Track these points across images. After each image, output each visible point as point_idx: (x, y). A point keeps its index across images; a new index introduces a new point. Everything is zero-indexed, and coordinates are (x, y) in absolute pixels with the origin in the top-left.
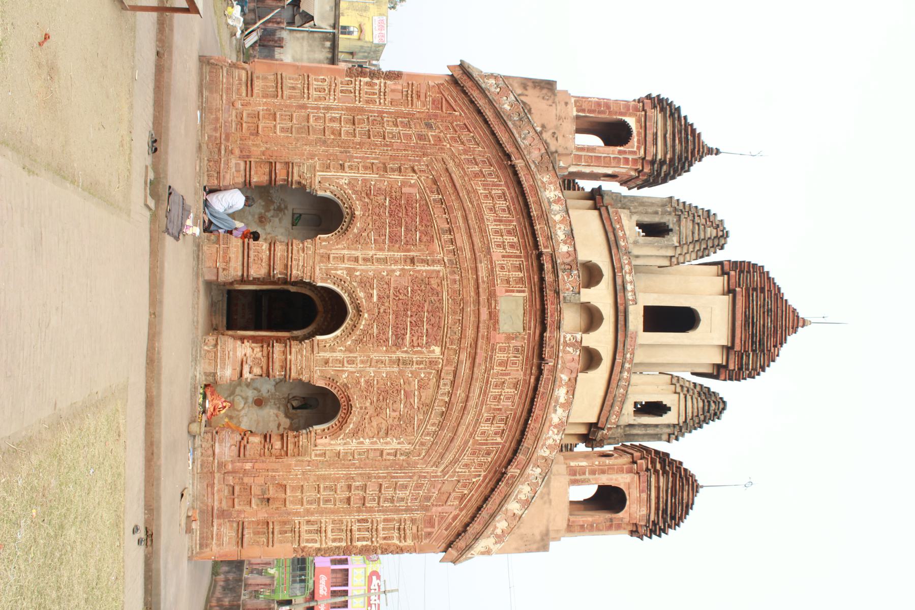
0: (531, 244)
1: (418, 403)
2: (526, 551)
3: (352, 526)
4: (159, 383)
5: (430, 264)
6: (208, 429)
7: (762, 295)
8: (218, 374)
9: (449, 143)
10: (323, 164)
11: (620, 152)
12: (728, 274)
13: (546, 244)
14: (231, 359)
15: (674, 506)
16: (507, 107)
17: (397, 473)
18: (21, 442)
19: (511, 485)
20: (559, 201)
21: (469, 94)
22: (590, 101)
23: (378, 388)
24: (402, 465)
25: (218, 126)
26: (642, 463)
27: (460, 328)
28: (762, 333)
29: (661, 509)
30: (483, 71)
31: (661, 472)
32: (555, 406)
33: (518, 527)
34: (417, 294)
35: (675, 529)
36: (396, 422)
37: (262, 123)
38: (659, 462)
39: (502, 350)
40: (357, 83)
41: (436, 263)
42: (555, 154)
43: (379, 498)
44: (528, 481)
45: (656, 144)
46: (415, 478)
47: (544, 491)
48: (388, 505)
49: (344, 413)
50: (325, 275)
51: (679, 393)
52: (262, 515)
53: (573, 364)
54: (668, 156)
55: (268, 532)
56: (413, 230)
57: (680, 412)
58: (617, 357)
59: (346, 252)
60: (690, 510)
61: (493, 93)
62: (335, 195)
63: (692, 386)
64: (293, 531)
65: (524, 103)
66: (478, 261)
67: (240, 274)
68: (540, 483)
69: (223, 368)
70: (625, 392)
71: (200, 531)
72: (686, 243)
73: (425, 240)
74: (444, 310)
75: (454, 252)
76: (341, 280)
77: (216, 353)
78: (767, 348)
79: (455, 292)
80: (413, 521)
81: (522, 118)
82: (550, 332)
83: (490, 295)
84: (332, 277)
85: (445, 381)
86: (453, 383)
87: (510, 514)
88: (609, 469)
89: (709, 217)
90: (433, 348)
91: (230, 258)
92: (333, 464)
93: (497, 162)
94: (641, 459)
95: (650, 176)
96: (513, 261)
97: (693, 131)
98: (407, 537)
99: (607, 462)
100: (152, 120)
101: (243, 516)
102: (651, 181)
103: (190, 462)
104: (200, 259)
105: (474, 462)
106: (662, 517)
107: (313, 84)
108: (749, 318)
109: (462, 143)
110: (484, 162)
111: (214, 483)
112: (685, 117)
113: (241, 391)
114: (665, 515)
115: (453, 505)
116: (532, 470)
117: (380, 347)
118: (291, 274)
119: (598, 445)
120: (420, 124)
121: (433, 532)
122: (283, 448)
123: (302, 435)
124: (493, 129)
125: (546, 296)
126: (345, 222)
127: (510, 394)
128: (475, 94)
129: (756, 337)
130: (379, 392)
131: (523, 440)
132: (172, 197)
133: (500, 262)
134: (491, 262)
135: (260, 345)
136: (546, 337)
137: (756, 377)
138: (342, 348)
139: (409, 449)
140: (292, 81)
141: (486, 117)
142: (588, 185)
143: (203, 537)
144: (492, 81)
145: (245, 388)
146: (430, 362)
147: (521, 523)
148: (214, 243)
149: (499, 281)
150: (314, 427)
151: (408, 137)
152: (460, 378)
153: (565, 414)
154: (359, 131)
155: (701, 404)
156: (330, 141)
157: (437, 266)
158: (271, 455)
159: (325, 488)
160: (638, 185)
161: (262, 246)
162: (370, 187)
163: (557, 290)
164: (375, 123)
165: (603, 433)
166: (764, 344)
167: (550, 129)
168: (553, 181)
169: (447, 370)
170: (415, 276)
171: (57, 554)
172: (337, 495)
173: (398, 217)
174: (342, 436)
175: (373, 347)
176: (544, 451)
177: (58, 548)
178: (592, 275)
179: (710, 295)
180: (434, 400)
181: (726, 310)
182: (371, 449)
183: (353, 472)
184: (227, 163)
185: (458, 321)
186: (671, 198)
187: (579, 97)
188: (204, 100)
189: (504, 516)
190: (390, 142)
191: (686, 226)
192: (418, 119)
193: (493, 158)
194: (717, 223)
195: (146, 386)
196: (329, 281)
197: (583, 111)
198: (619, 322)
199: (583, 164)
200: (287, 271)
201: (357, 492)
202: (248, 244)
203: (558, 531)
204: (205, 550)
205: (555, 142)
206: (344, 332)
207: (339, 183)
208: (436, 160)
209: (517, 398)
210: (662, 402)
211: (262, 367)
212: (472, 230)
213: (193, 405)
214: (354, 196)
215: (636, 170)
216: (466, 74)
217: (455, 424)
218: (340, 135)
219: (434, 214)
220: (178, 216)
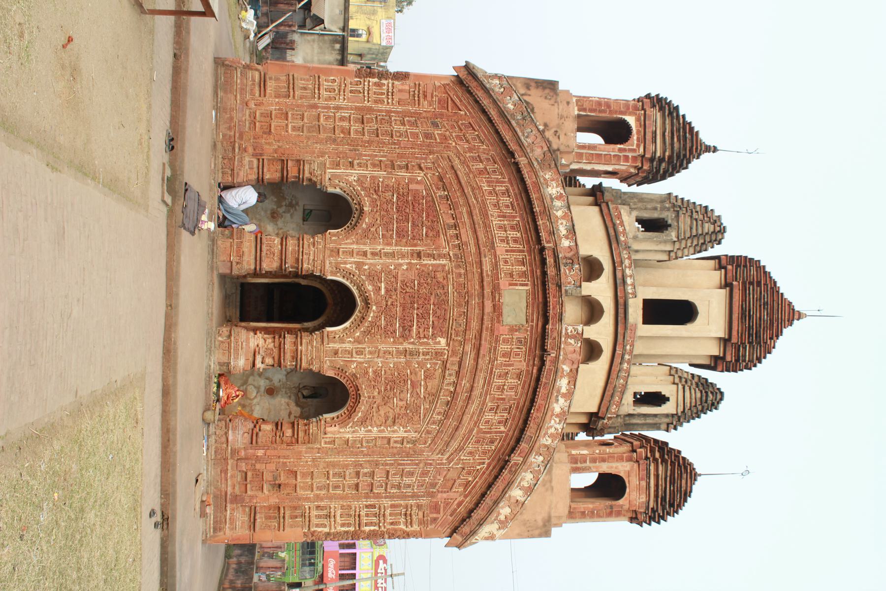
0: (534, 239)
1: (424, 392)
2: (528, 537)
4: (175, 372)
5: (436, 258)
6: (221, 417)
7: (759, 288)
8: (232, 364)
9: (454, 141)
10: (333, 161)
11: (620, 150)
12: (725, 268)
13: (548, 239)
15: (672, 493)
16: (510, 106)
18: (44, 428)
19: (515, 473)
21: (474, 94)
22: (591, 101)
23: (386, 378)
24: (409, 452)
25: (233, 124)
27: (464, 320)
28: (758, 326)
29: (660, 496)
31: (660, 460)
32: (557, 396)
34: (423, 287)
35: (673, 516)
36: (403, 411)
37: (274, 122)
38: (658, 451)
39: (506, 341)
40: (366, 83)
41: (442, 258)
42: (557, 152)
43: (387, 484)
45: (655, 142)
46: (421, 465)
47: (546, 479)
48: (395, 491)
49: (353, 402)
50: (334, 268)
52: (274, 501)
54: (667, 154)
55: (279, 517)
57: (679, 402)
58: (617, 349)
59: (355, 246)
60: (688, 498)
61: (497, 93)
62: (345, 192)
64: (303, 516)
65: (527, 103)
66: (483, 256)
67: (253, 267)
68: (542, 470)
69: (236, 358)
71: (214, 516)
72: (684, 238)
73: (431, 235)
75: (459, 246)
76: (350, 273)
77: (229, 344)
80: (419, 507)
81: (525, 117)
82: (552, 324)
83: (494, 288)
84: (342, 270)
85: (451, 372)
86: (458, 373)
87: (513, 501)
88: (609, 457)
89: (706, 212)
90: (439, 339)
91: (243, 252)
92: (342, 451)
93: (501, 159)
94: (640, 448)
95: (649, 173)
96: (516, 255)
97: (691, 129)
98: (413, 522)
99: (608, 450)
100: (169, 120)
102: (651, 178)
103: (205, 449)
104: (215, 253)
105: (478, 450)
107: (323, 84)
108: (746, 311)
109: (467, 141)
110: (488, 159)
111: (227, 470)
112: (684, 116)
113: (254, 380)
114: (663, 503)
115: (457, 492)
116: (534, 458)
117: (387, 338)
118: (302, 268)
120: (426, 123)
121: (438, 518)
123: (312, 423)
124: (497, 127)
125: (549, 289)
126: (354, 217)
128: (480, 94)
131: (526, 429)
132: (188, 193)
133: (503, 257)
134: (495, 256)
135: (272, 336)
136: (548, 329)
138: (351, 339)
139: (415, 437)
140: (303, 82)
141: (491, 116)
142: (589, 182)
143: (217, 521)
144: (497, 82)
145: (257, 378)
146: (436, 353)
148: (228, 238)
152: (465, 369)
153: (567, 404)
154: (368, 129)
155: (699, 395)
157: (443, 261)
159: (335, 475)
160: (638, 182)
162: (378, 184)
163: (559, 284)
164: (383, 121)
165: (603, 423)
166: (760, 337)
167: (552, 128)
168: (555, 178)
171: (78, 537)
172: (346, 481)
173: (405, 212)
175: (381, 338)
176: (547, 440)
177: (79, 530)
178: (592, 269)
179: (708, 288)
180: (439, 389)
182: (379, 437)
183: (362, 459)
184: (241, 160)
185: (463, 313)
186: (670, 194)
187: (580, 97)
188: (219, 100)
189: (507, 502)
190: (398, 140)
191: (685, 222)
192: (424, 118)
193: (497, 156)
194: (714, 218)
195: (163, 375)
196: (338, 274)
197: (585, 110)
198: (619, 315)
199: (584, 161)
201: (365, 479)
202: (261, 238)
203: (559, 517)
204: (219, 534)
205: (558, 140)
206: (353, 323)
207: (348, 180)
208: (442, 158)
209: (520, 388)
210: (661, 392)
211: (274, 358)
212: (477, 226)
213: (207, 394)
214: (362, 192)
215: (635, 167)
216: (471, 74)
217: (460, 413)
218: (349, 133)
219: (440, 210)
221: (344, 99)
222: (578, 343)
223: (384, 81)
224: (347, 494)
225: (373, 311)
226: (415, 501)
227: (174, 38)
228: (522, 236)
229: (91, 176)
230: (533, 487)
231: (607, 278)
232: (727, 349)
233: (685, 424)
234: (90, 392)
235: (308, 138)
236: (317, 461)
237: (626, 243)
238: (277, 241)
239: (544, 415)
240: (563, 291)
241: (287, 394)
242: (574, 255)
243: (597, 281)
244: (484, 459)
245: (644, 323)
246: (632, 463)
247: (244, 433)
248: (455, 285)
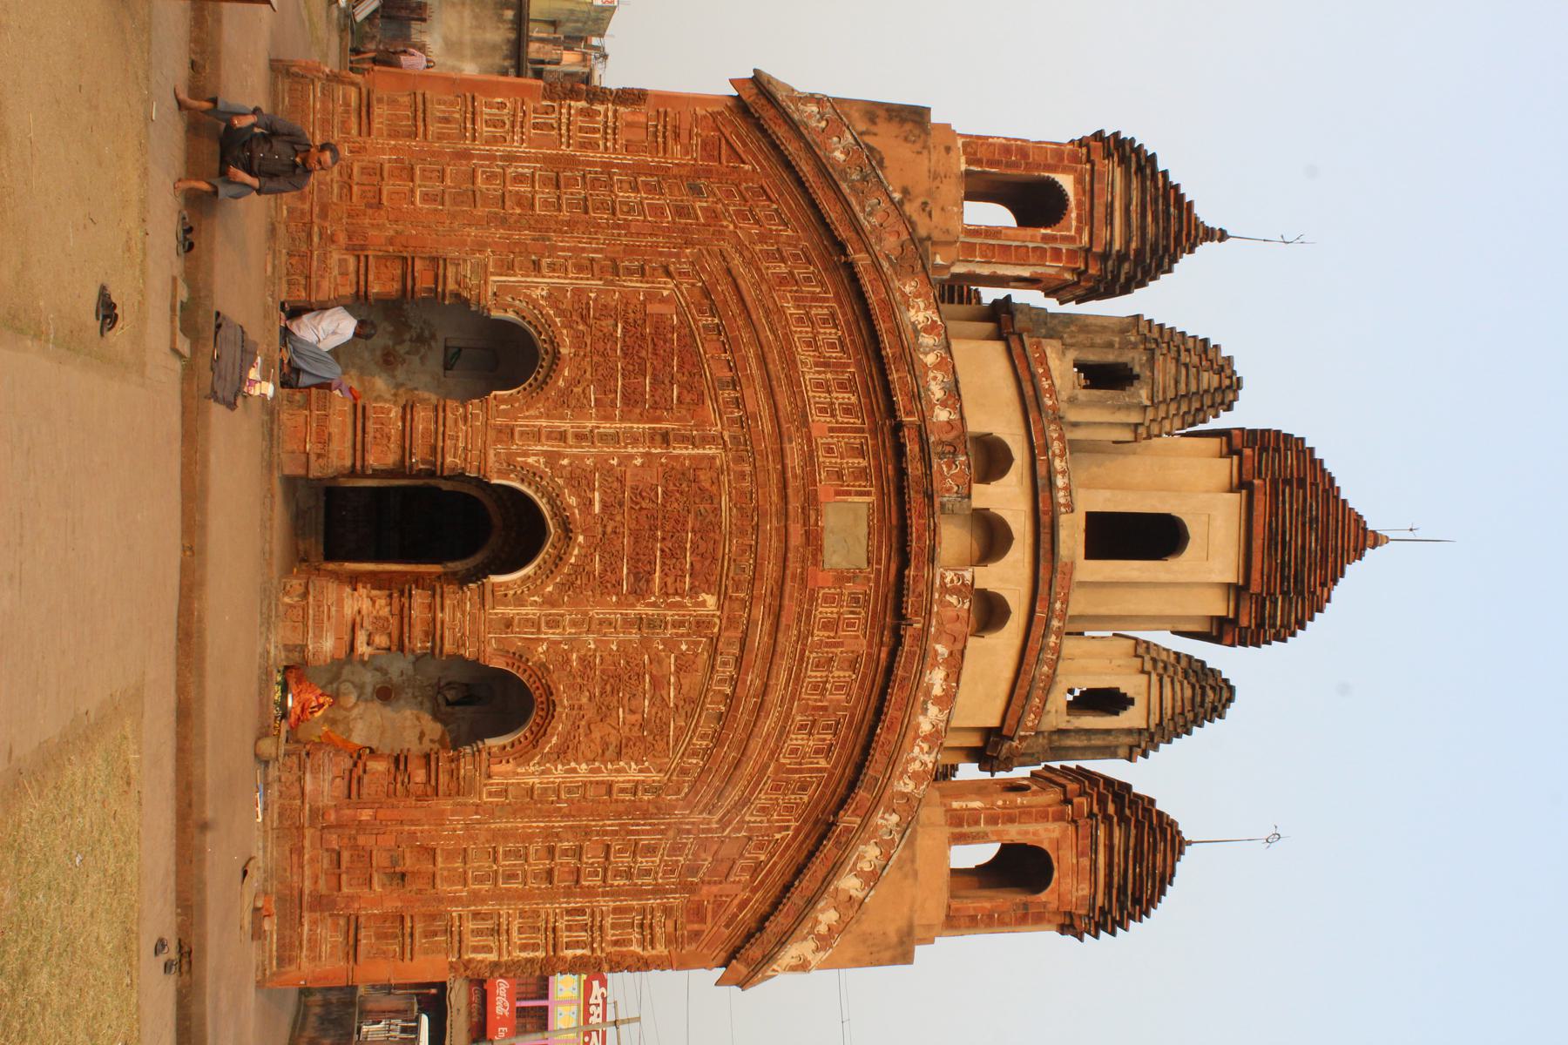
0: (882, 406)
1: (675, 696)
2: (872, 964)
3: (555, 922)
4: (201, 675)
5: (697, 443)
6: (291, 747)
7: (1301, 491)
8: (310, 647)
10: (502, 260)
11: (1045, 238)
12: (1239, 453)
13: (909, 407)
14: (333, 620)
15: (1139, 880)
16: (839, 155)
17: (638, 825)
19: (845, 845)
21: (770, 131)
22: (991, 144)
23: (603, 672)
24: (648, 809)
26: (1083, 803)
27: (751, 562)
29: (1115, 886)
30: (795, 87)
31: (1115, 819)
32: (925, 702)
33: (857, 922)
35: (1140, 921)
36: (636, 733)
37: (388, 185)
38: (1112, 801)
39: (829, 600)
40: (564, 111)
41: (709, 443)
43: (605, 870)
46: (671, 833)
48: (622, 883)
49: (542, 717)
50: (505, 464)
51: (1149, 674)
52: (392, 904)
53: (958, 625)
54: (1133, 245)
55: (403, 935)
56: (666, 382)
57: (1152, 707)
58: (1038, 609)
59: (543, 423)
61: (814, 129)
62: (524, 318)
63: (1172, 658)
64: (448, 931)
65: (871, 149)
66: (786, 439)
67: (348, 463)
69: (318, 637)
70: (1051, 671)
72: (1164, 401)
75: (742, 422)
76: (535, 474)
78: (1309, 587)
79: (742, 493)
80: (667, 911)
82: (916, 567)
83: (807, 499)
84: (519, 469)
85: (725, 658)
86: (739, 661)
87: (843, 897)
90: (703, 596)
91: (330, 434)
93: (821, 256)
94: (1080, 795)
96: (849, 438)
97: (1180, 198)
98: (656, 940)
99: (1019, 800)
101: (356, 905)
102: (1102, 290)
103: (259, 809)
104: (275, 437)
105: (778, 804)
107: (481, 112)
109: (757, 222)
111: (303, 847)
112: (1165, 173)
113: (353, 673)
114: (1122, 898)
115: (739, 882)
116: (883, 818)
118: (443, 463)
119: (1002, 766)
122: (429, 781)
123: (464, 757)
124: (814, 196)
125: (910, 503)
126: (542, 367)
127: (842, 679)
128: (781, 132)
130: (605, 677)
131: (867, 763)
132: (221, 332)
133: (824, 440)
134: (809, 440)
135: (387, 592)
137: (1289, 639)
138: (536, 598)
139: (659, 782)
140: (443, 107)
141: (801, 174)
142: (989, 295)
143: (284, 945)
145: (359, 667)
146: (698, 623)
148: (300, 407)
150: (486, 740)
151: (658, 211)
152: (751, 651)
153: (943, 717)
154: (567, 199)
155: (1188, 693)
156: (514, 218)
157: (710, 449)
158: (408, 793)
159: (507, 854)
160: (1078, 296)
161: (390, 411)
162: (588, 303)
163: (930, 492)
165: (1011, 746)
167: (917, 197)
169: (730, 638)
170: (670, 466)
171: (16, 1024)
173: (639, 357)
174: (537, 759)
175: (594, 596)
176: (905, 784)
177: (18, 1012)
181: (1236, 519)
182: (591, 782)
183: (558, 824)
184: (324, 258)
185: (748, 549)
186: (1137, 317)
187: (971, 136)
190: (625, 220)
191: (1165, 371)
193: (814, 249)
194: (1220, 362)
195: (178, 681)
196: (512, 476)
197: (978, 162)
199: (978, 259)
200: (436, 457)
201: (565, 860)
203: (929, 927)
204: (288, 968)
205: (927, 219)
206: (540, 568)
209: (855, 686)
210: (1117, 689)
211: (390, 635)
212: (774, 383)
214: (558, 320)
215: (1074, 270)
217: (744, 736)
218: (532, 206)
219: (705, 353)
220: (234, 365)
221: (522, 141)
222: (964, 603)
223: (601, 108)
224: (531, 889)
225: (579, 545)
226: (658, 901)
227: (191, 32)
228: (860, 401)
229: (32, 333)
230: (879, 872)
231: (1019, 476)
232: (1242, 604)
233: (1162, 746)
234: (37, 744)
235: (454, 216)
236: (473, 829)
237: (1055, 409)
238: (395, 413)
239: (901, 737)
240: (937, 505)
241: (415, 697)
242: (959, 437)
243: (1002, 481)
244: (789, 821)
245: (1087, 557)
246: (1064, 824)
247: (334, 778)
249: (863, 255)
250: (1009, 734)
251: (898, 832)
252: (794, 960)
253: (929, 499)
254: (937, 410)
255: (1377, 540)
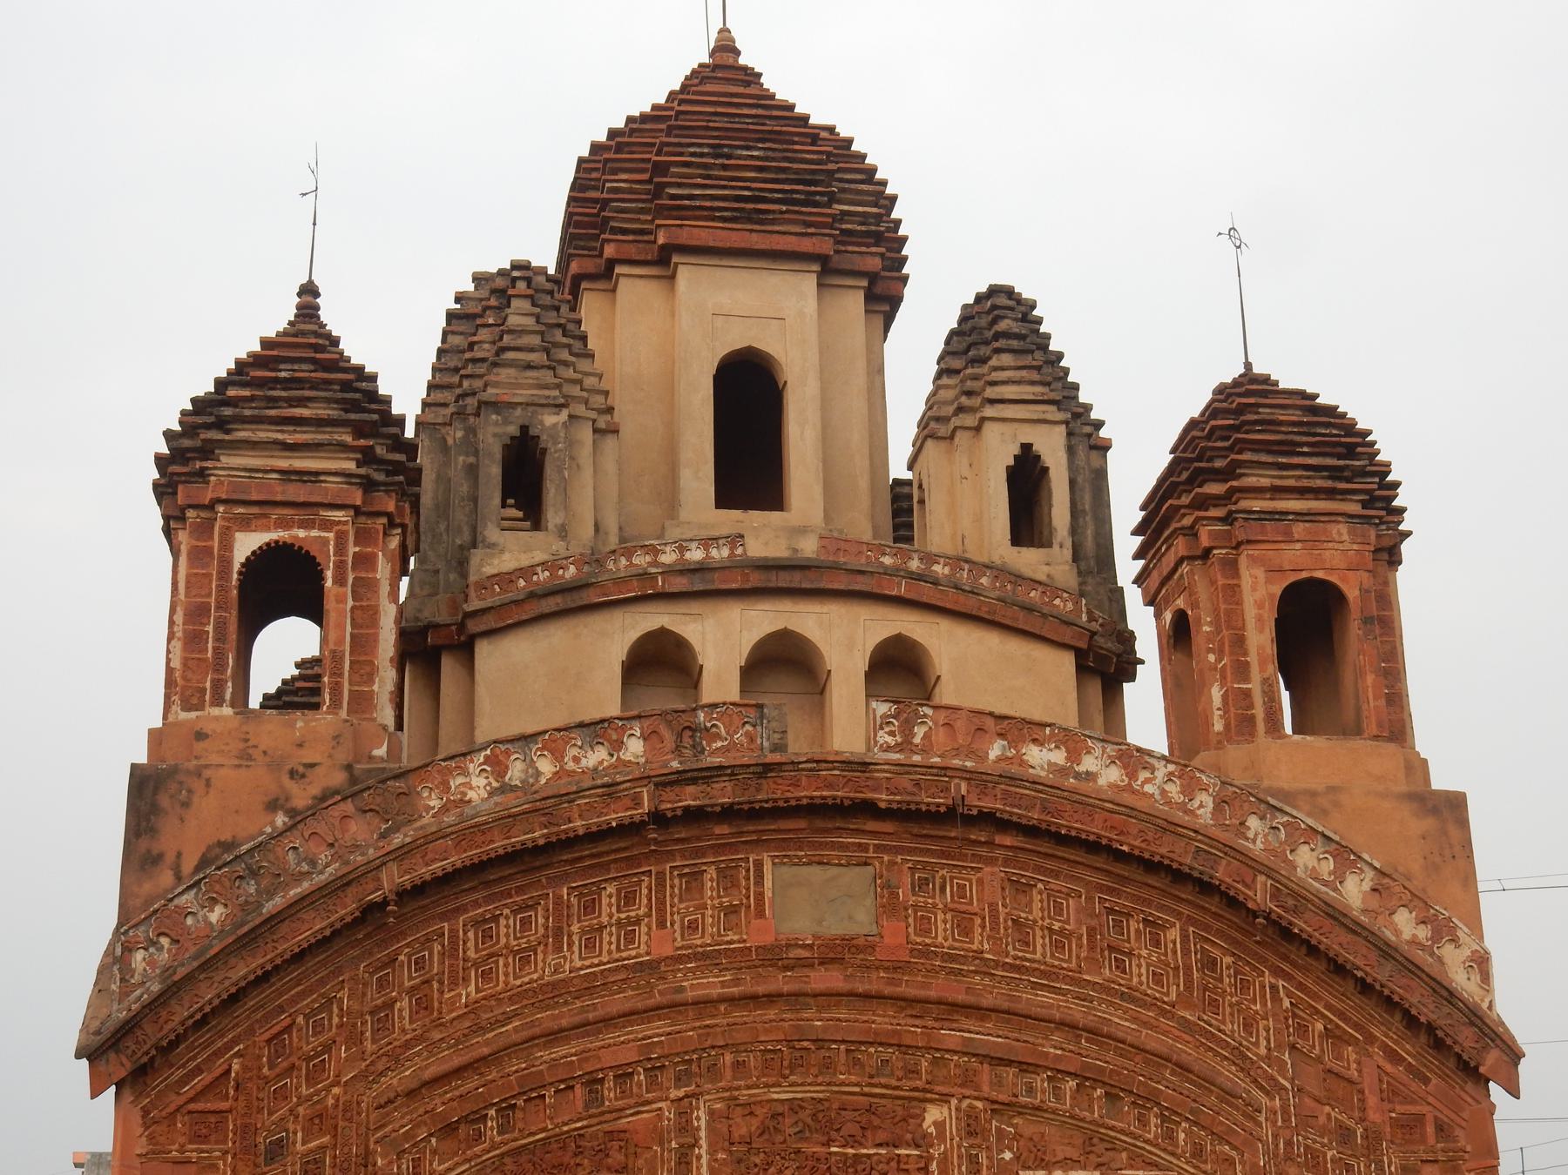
0: (622, 845)
9: (328, 1089)
11: (340, 580)
12: (611, 263)
15: (1319, 449)
16: (216, 915)
19: (1299, 898)
20: (499, 763)
27: (872, 1050)
29: (1329, 484)
32: (1077, 776)
42: (356, 772)
44: (1285, 851)
45: (317, 473)
51: (983, 420)
53: (959, 724)
54: (348, 439)
61: (174, 957)
65: (203, 863)
66: (679, 997)
68: (1285, 819)
73: (620, 1157)
74: (821, 1096)
75: (654, 1068)
78: (819, 162)
79: (767, 1066)
81: (249, 868)
82: (875, 790)
85: (1021, 1088)
86: (1025, 1067)
87: (1374, 903)
88: (1228, 628)
93: (384, 943)
94: (1196, 535)
97: (255, 361)
99: (1206, 628)
105: (1239, 1003)
106: (1348, 481)
109: (327, 1048)
110: (382, 984)
115: (1359, 1063)
116: (1254, 841)
121: (1436, 1118)
125: (775, 801)
127: (1045, 904)
128: (181, 1012)
129: (793, 191)
131: (1175, 866)
133: (678, 935)
134: (679, 959)
136: (890, 802)
141: (252, 977)
147: (1396, 870)
149: (731, 936)
155: (1006, 359)
157: (698, 1118)
166: (813, 172)
168: (439, 778)
176: (1201, 806)
181: (719, 272)
185: (851, 1055)
187: (167, 697)
191: (509, 384)
193: (371, 954)
198: (795, 585)
205: (317, 769)
209: (1055, 884)
212: (591, 1016)
216: (119, 1040)
222: (925, 716)
228: (614, 879)
230: (1334, 846)
231: (688, 618)
232: (849, 267)
239: (1134, 813)
243: (697, 646)
244: (1263, 987)
246: (1243, 561)
248: (771, 1080)
249: (384, 876)
250: (1087, 639)
251: (1274, 817)
252: (1472, 978)
253: (771, 771)
254: (626, 756)
255: (725, 47)
